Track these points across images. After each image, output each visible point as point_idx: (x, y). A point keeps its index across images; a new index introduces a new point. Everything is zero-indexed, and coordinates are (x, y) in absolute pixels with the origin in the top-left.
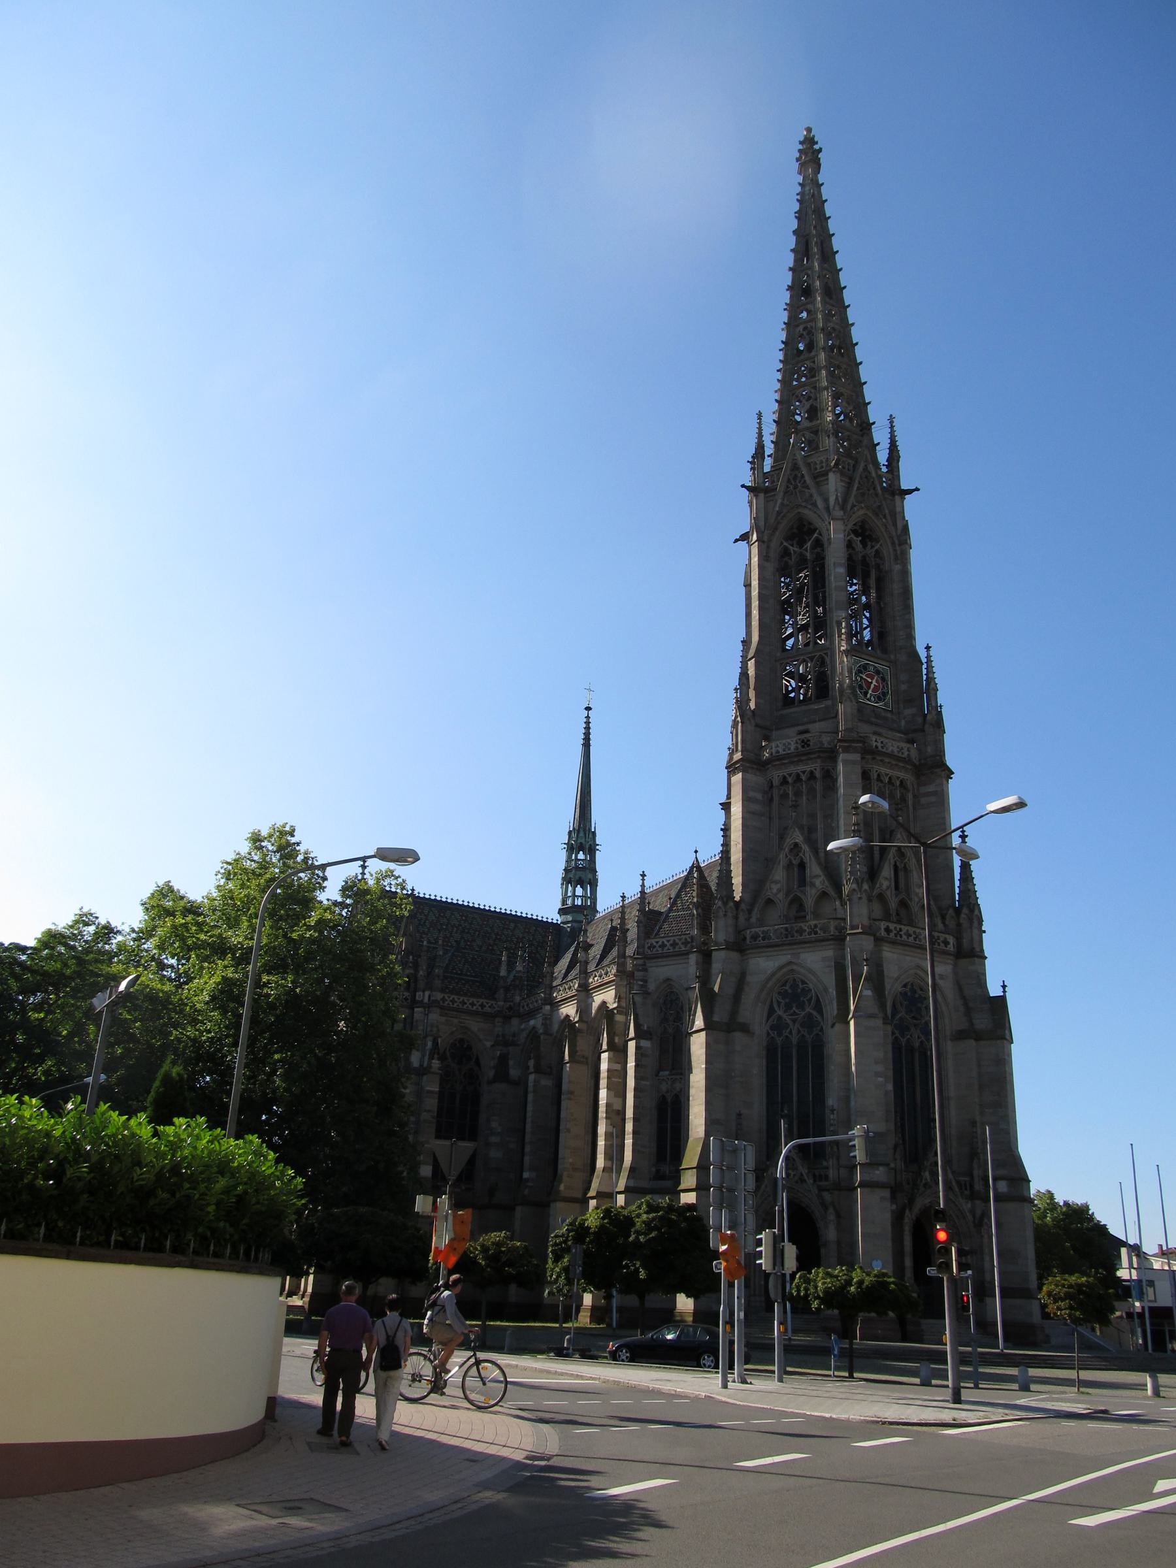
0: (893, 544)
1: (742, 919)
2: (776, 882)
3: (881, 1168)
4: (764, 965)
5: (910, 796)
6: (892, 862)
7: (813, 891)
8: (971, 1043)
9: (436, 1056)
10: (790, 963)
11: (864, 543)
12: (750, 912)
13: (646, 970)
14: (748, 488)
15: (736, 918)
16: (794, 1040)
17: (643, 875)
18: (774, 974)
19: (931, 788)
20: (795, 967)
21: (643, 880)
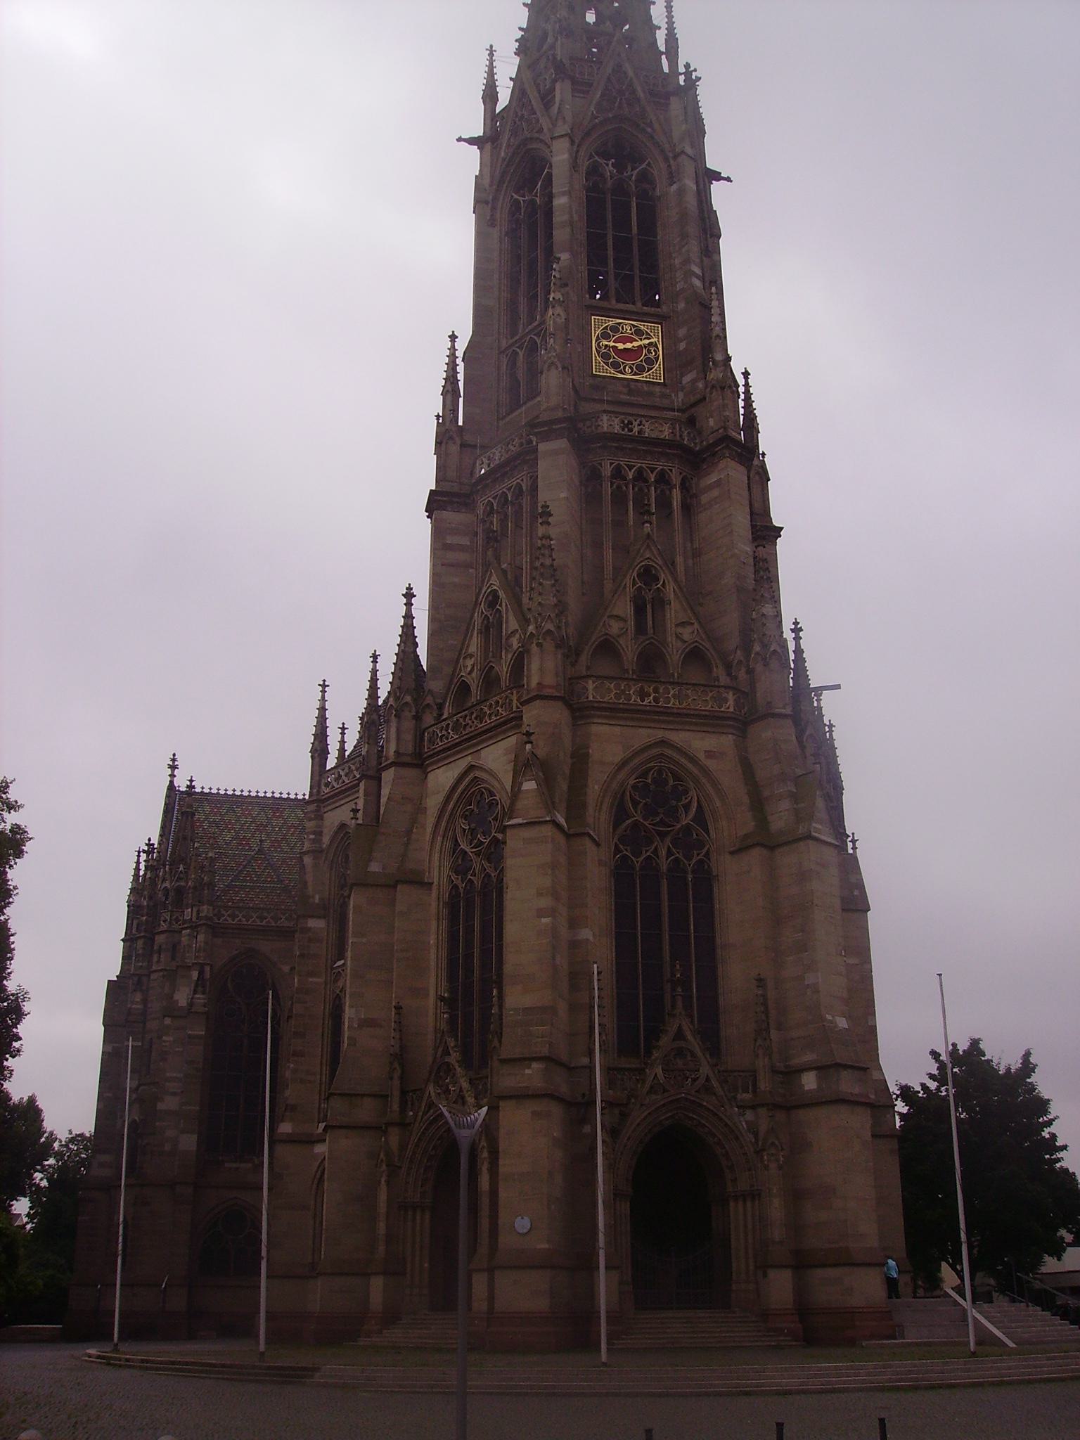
0: (666, 159)
1: (429, 719)
2: (471, 656)
3: (535, 1065)
4: (443, 778)
5: (676, 496)
6: (630, 590)
7: (510, 656)
8: (756, 852)
9: (200, 989)
10: (471, 768)
11: (620, 167)
12: (440, 707)
13: (321, 818)
14: (471, 141)
15: (417, 718)
16: (478, 883)
17: (324, 686)
18: (454, 788)
19: (713, 478)
20: (477, 774)
21: (324, 692)
